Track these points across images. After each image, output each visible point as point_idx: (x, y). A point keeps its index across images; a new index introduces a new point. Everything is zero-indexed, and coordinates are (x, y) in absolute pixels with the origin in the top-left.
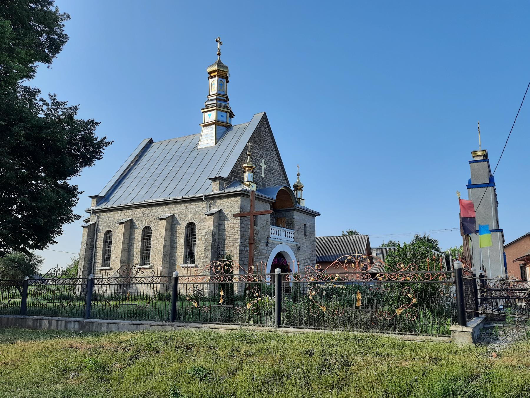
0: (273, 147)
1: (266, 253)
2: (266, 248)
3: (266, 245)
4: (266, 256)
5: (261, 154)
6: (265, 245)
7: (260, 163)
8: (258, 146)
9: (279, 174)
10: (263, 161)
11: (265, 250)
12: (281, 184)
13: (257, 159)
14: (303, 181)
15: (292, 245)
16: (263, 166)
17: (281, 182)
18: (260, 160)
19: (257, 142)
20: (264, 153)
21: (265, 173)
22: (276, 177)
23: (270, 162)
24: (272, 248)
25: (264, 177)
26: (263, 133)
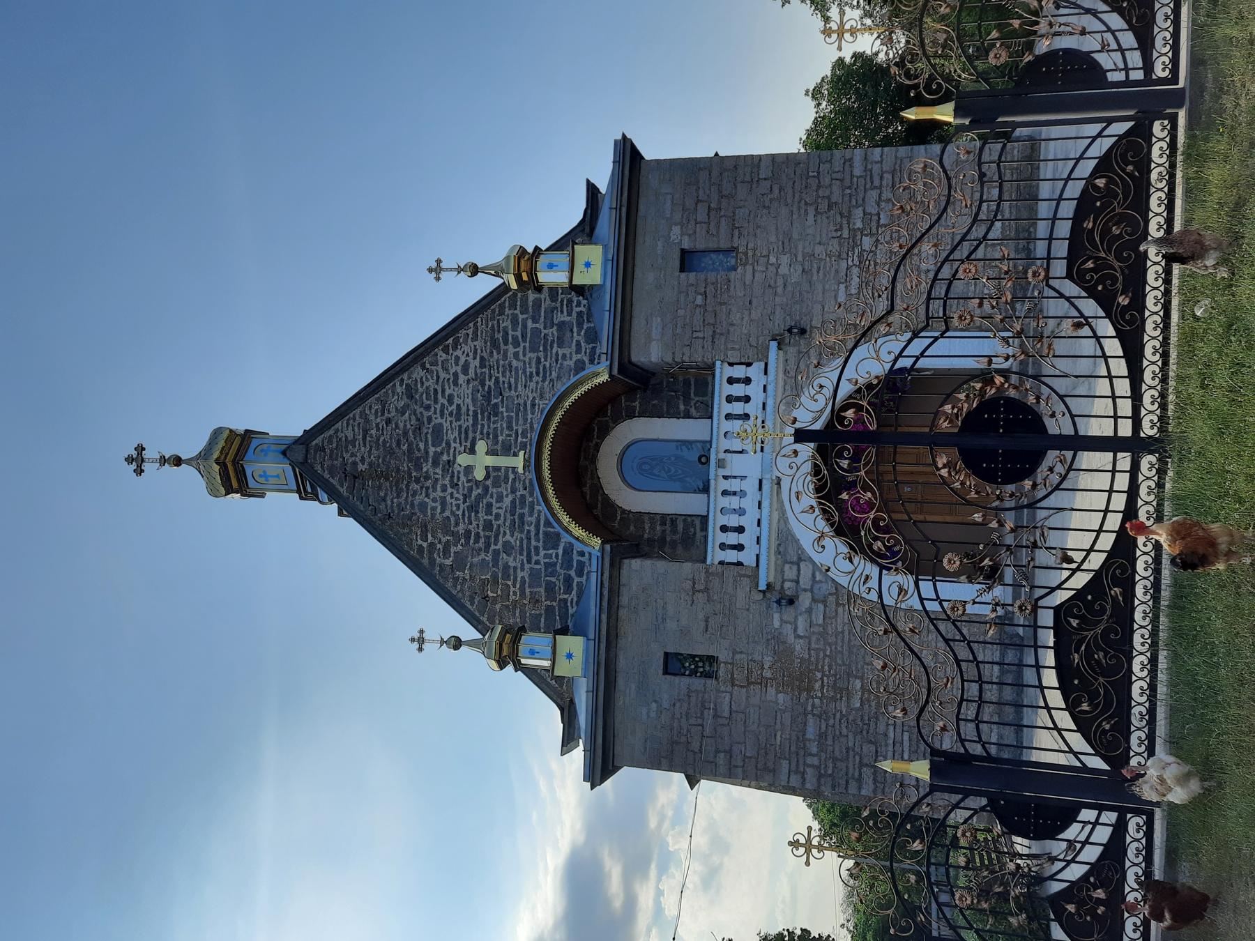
0: (399, 390)
1: (824, 602)
2: (805, 600)
3: (791, 602)
4: (838, 604)
5: (439, 471)
6: (789, 613)
7: (477, 483)
8: (415, 493)
9: (495, 344)
10: (463, 460)
11: (809, 611)
12: (530, 324)
13: (465, 497)
14: (495, 252)
15: (781, 383)
16: (482, 460)
17: (525, 326)
18: (463, 479)
19: (402, 500)
20: (432, 450)
21: (507, 450)
22: (511, 366)
23: (458, 406)
24: (800, 559)
25: (522, 453)
26: (363, 460)
